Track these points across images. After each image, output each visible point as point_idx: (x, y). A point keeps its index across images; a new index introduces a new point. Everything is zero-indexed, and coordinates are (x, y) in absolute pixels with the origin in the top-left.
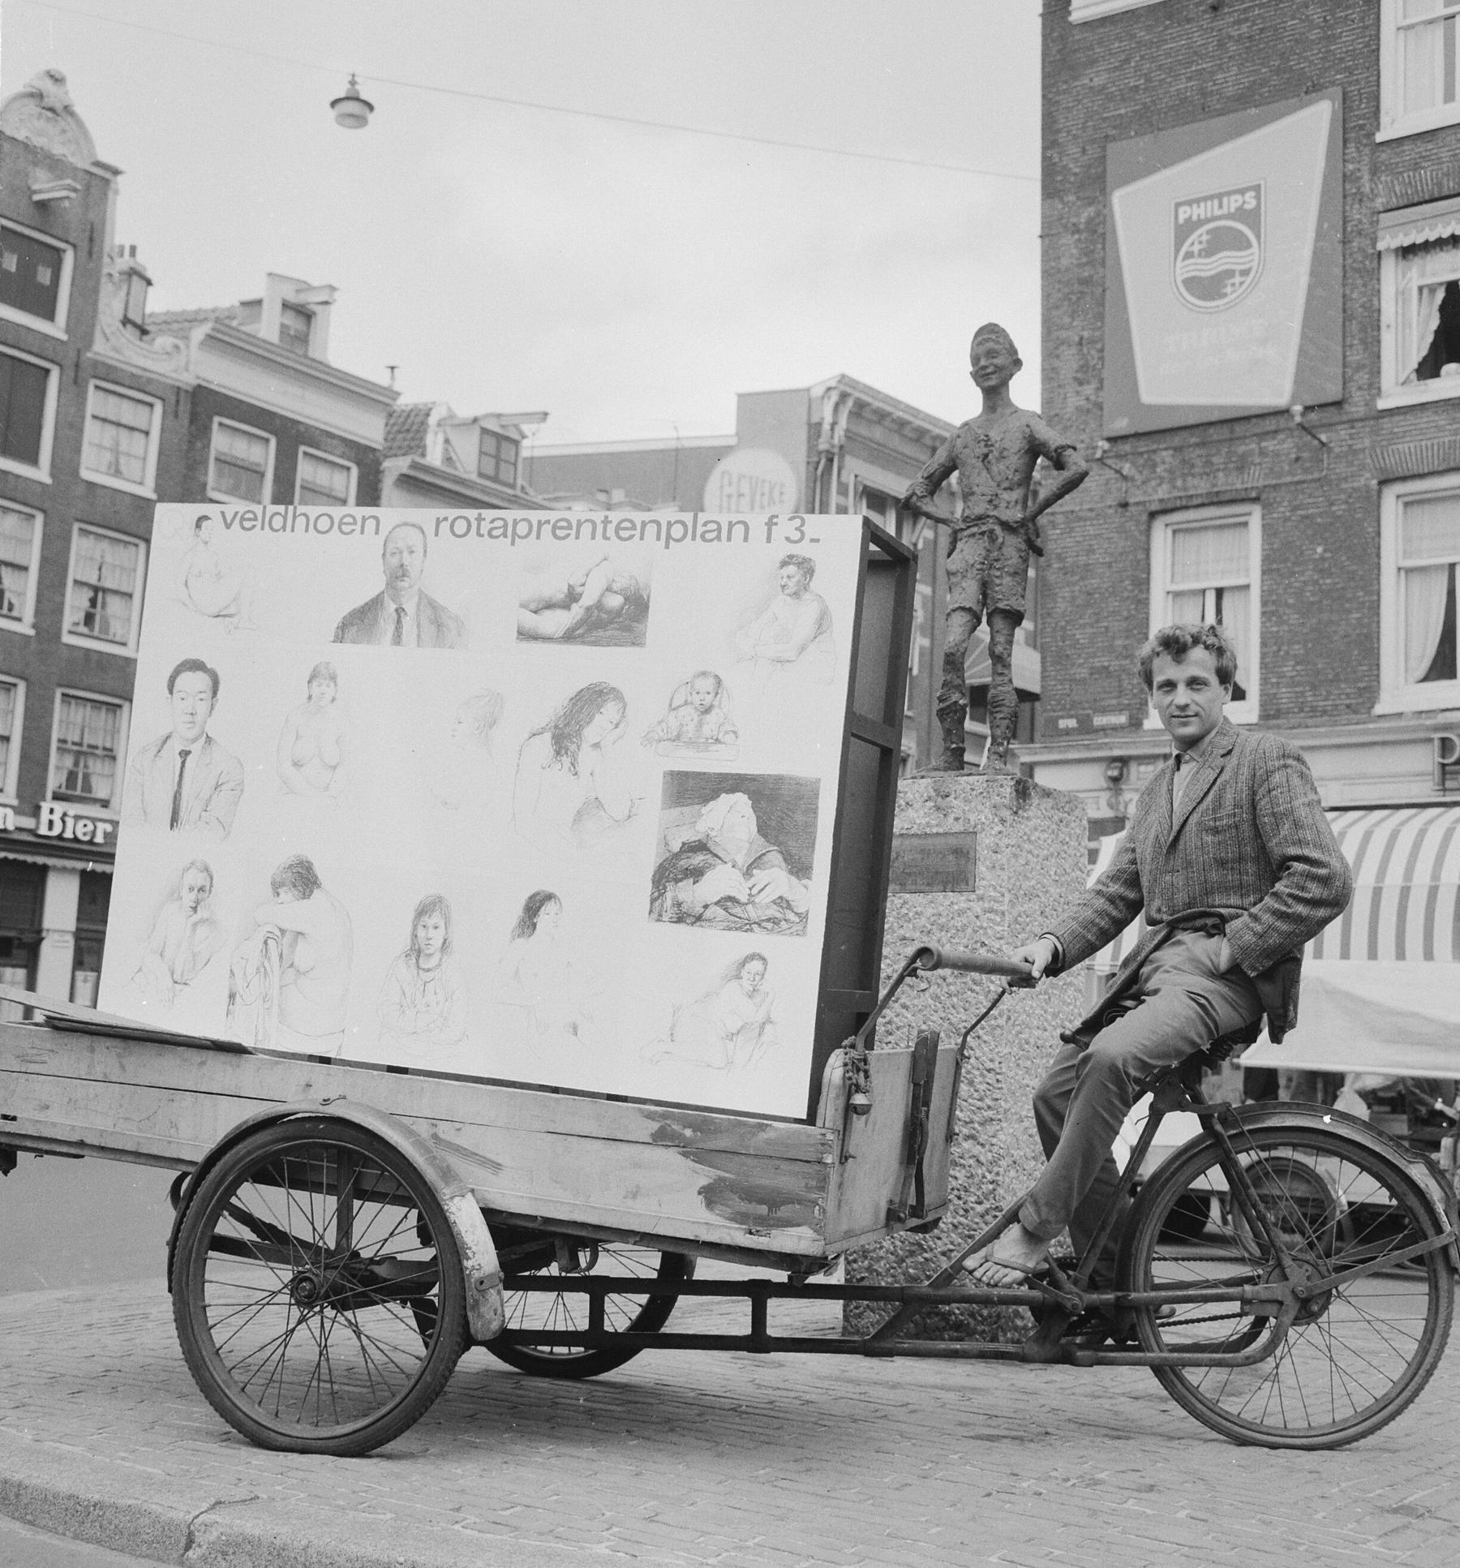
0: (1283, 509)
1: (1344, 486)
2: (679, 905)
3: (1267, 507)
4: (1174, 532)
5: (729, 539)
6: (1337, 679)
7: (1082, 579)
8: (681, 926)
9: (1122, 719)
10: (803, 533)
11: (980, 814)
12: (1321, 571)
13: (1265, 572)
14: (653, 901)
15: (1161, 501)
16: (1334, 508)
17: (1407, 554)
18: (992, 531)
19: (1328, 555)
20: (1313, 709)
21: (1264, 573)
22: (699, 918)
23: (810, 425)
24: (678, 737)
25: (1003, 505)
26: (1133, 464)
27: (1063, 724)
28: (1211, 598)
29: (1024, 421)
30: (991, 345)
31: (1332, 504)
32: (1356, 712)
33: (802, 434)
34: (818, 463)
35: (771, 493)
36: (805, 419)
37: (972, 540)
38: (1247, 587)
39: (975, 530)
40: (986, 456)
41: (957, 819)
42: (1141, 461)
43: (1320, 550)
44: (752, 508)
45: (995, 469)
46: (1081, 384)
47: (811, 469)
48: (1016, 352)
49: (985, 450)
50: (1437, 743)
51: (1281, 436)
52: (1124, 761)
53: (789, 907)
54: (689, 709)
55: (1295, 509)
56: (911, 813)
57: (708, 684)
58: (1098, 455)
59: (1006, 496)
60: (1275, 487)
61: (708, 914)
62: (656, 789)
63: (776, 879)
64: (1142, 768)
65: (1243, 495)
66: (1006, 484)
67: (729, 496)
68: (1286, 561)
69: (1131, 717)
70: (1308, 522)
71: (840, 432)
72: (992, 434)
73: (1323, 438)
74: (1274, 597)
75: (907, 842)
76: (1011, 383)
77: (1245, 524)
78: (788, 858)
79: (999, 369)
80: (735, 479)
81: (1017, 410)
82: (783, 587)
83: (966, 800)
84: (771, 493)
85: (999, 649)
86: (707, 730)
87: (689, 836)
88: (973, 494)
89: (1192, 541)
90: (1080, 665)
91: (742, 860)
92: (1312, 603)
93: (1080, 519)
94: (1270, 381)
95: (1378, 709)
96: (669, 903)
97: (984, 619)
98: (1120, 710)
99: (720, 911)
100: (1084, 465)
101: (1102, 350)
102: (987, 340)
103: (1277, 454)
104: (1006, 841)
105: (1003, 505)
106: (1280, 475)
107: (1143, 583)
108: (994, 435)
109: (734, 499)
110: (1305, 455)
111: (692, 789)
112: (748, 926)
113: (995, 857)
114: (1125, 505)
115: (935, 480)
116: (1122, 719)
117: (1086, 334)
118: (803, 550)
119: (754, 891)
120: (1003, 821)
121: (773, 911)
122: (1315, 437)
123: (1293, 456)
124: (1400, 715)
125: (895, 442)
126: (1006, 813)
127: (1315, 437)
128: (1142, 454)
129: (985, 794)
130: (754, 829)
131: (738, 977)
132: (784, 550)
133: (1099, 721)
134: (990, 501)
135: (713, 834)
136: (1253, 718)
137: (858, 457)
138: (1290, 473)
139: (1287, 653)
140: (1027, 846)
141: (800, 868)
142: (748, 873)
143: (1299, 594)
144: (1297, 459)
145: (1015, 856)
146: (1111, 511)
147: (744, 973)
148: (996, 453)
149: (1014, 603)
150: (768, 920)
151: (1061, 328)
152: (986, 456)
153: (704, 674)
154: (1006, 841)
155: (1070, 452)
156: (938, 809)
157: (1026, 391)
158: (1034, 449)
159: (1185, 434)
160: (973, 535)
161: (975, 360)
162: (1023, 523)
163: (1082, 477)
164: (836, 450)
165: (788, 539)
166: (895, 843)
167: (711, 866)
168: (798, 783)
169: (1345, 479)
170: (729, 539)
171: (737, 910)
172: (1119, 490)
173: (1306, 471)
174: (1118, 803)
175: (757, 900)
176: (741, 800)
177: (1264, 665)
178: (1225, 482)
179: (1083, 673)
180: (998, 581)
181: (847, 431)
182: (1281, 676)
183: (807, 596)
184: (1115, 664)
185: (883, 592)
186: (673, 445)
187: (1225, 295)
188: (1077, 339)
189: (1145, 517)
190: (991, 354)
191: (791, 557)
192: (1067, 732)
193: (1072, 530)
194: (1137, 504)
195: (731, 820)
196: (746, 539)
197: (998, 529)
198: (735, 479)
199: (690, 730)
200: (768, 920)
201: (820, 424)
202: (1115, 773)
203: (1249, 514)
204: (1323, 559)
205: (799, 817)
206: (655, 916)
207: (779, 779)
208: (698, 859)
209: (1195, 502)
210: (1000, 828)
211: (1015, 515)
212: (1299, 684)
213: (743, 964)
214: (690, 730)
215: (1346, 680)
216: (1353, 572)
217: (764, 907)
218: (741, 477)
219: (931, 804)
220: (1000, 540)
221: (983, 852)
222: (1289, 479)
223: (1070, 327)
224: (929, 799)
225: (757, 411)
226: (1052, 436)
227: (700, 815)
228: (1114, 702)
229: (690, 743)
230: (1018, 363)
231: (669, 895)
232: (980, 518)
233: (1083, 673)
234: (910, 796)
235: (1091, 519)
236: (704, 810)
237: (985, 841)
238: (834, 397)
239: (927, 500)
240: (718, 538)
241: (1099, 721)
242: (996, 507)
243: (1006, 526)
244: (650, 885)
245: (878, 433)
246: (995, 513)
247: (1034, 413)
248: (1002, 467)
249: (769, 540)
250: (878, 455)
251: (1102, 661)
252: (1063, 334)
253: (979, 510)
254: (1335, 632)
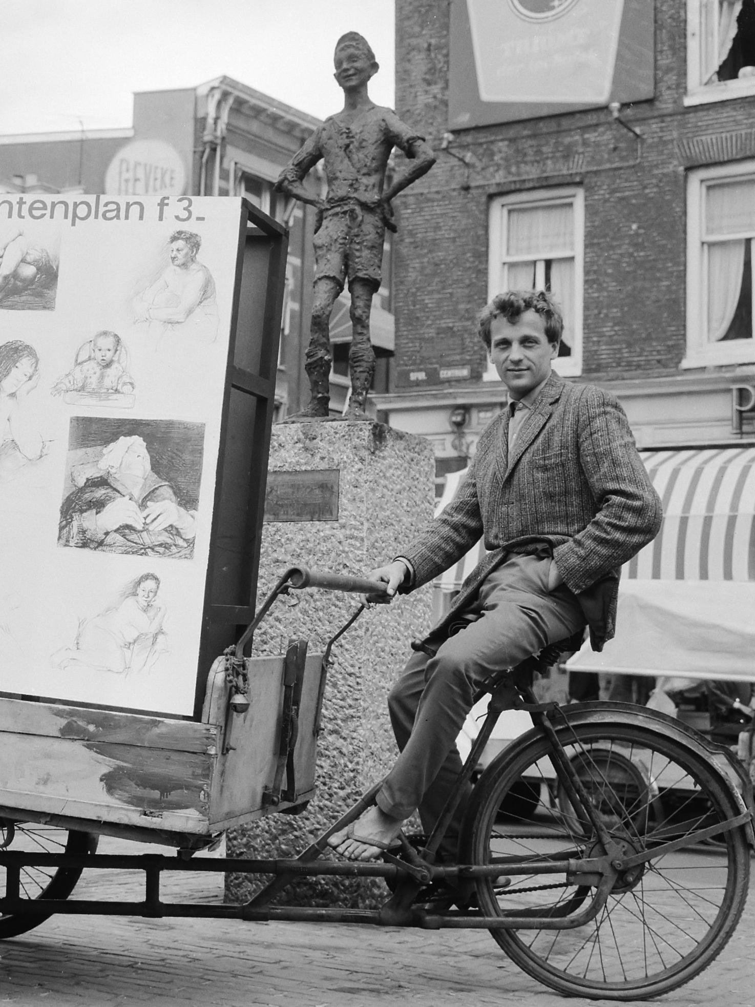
0: (603, 192)
1: (656, 172)
2: (84, 532)
3: (590, 190)
4: (510, 212)
5: (127, 218)
6: (649, 338)
7: (430, 251)
8: (86, 551)
9: (465, 372)
10: (190, 213)
11: (343, 454)
12: (636, 245)
14: (61, 528)
15: (498, 184)
16: (647, 191)
17: (709, 231)
18: (352, 211)
19: (642, 231)
20: (629, 364)
21: (586, 246)
22: (101, 544)
23: (196, 120)
24: (83, 388)
25: (362, 188)
26: (474, 153)
29: (380, 117)
30: (352, 51)
31: (645, 188)
32: (665, 366)
33: (190, 127)
34: (203, 152)
35: (162, 178)
36: (191, 114)
37: (336, 219)
38: (572, 259)
39: (338, 209)
40: (348, 146)
41: (322, 458)
42: (481, 151)
43: (634, 227)
44: (147, 191)
45: (355, 157)
46: (429, 83)
47: (197, 157)
48: (373, 57)
49: (347, 141)
50: (735, 393)
51: (601, 129)
53: (178, 534)
54: (92, 364)
55: (613, 191)
56: (283, 453)
57: (109, 342)
58: (444, 145)
59: (364, 180)
60: (596, 173)
61: (109, 540)
62: (64, 432)
63: (167, 509)
64: (482, 415)
65: (569, 180)
66: (365, 171)
67: (127, 181)
68: (605, 236)
69: (472, 371)
70: (624, 203)
71: (222, 125)
72: (352, 127)
73: (638, 130)
74: (595, 268)
75: (280, 478)
76: (369, 83)
77: (570, 205)
78: (177, 492)
79: (358, 71)
80: (132, 166)
81: (374, 107)
82: (173, 259)
83: (331, 443)
84: (162, 178)
85: (359, 312)
86: (108, 382)
87: (92, 472)
88: (336, 178)
89: (524, 220)
90: (429, 326)
91: (138, 493)
92: (628, 272)
93: (428, 200)
94: (593, 84)
95: (685, 364)
96: (75, 530)
97: (346, 287)
98: (463, 365)
99: (119, 538)
100: (431, 154)
101: (447, 55)
102: (348, 47)
103: (597, 145)
104: (365, 477)
105: (362, 188)
106: (600, 163)
107: (483, 256)
108: (355, 128)
109: (131, 184)
110: (622, 145)
111: (94, 433)
112: (143, 550)
113: (355, 491)
114: (467, 188)
115: (303, 167)
117: (433, 41)
118: (190, 227)
119: (148, 521)
120: (362, 460)
121: (165, 538)
122: (630, 130)
123: (612, 146)
124: (703, 369)
125: (270, 134)
126: (365, 454)
127: (630, 130)
128: (481, 144)
129: (347, 437)
130: (149, 467)
131: (135, 594)
132: (171, 226)
133: (445, 374)
134: (351, 185)
135: (113, 471)
136: (578, 372)
137: (237, 147)
138: (610, 161)
139: (606, 315)
140: (383, 482)
141: (188, 501)
142: (143, 505)
144: (615, 149)
145: (373, 490)
146: (455, 193)
147: (140, 591)
148: (356, 144)
149: (372, 273)
150: (160, 545)
151: (412, 36)
152: (348, 146)
153: (105, 333)
154: (365, 477)
155: (419, 142)
156: (306, 449)
157: (382, 90)
158: (389, 140)
159: (518, 127)
160: (337, 214)
161: (338, 63)
162: (379, 204)
163: (431, 163)
164: (219, 141)
165: (177, 217)
166: (270, 479)
167: (111, 499)
168: (186, 427)
169: (656, 166)
170: (127, 218)
171: (134, 537)
172: (462, 175)
173: (622, 159)
174: (461, 445)
175: (151, 528)
176: (137, 443)
177: (586, 326)
178: (554, 168)
179: (431, 332)
180: (357, 254)
181: (228, 124)
182: (601, 335)
183: (194, 266)
184: (458, 326)
185: (259, 264)
186: (78, 136)
187: (553, 8)
188: (426, 45)
189: (484, 199)
190: (352, 58)
191: (180, 233)
192: (418, 383)
193: (422, 209)
194: (478, 187)
195: (129, 459)
196: (141, 218)
197: (358, 209)
198: (132, 166)
199: (93, 382)
200: (160, 545)
201: (204, 119)
202: (459, 419)
203: (574, 196)
204: (637, 235)
205: (187, 457)
206: (63, 541)
207: (170, 424)
208: (100, 493)
209: (531, 185)
210: (359, 466)
211: (373, 197)
212: (617, 342)
213: (139, 583)
214: (93, 382)
215: (657, 339)
216: (664, 246)
217: (156, 534)
218: (137, 164)
219: (300, 445)
220: (360, 218)
221: (345, 487)
222: (608, 166)
223: (419, 35)
224: (299, 441)
225: (152, 107)
226: (405, 130)
227: (102, 455)
228: (458, 357)
229: (93, 393)
230: (375, 66)
231: (75, 524)
232: (342, 199)
233: (431, 332)
234: (282, 438)
235: (438, 200)
236: (105, 451)
237: (347, 477)
238: (217, 95)
239: (297, 184)
240: (118, 217)
241: (445, 374)
242: (356, 190)
243: (364, 206)
244: (59, 515)
245: (255, 127)
246: (355, 195)
247: (389, 110)
248: (361, 155)
249: (161, 219)
250: (255, 145)
251: (447, 322)
252: (414, 41)
253: (342, 192)
254: (648, 298)
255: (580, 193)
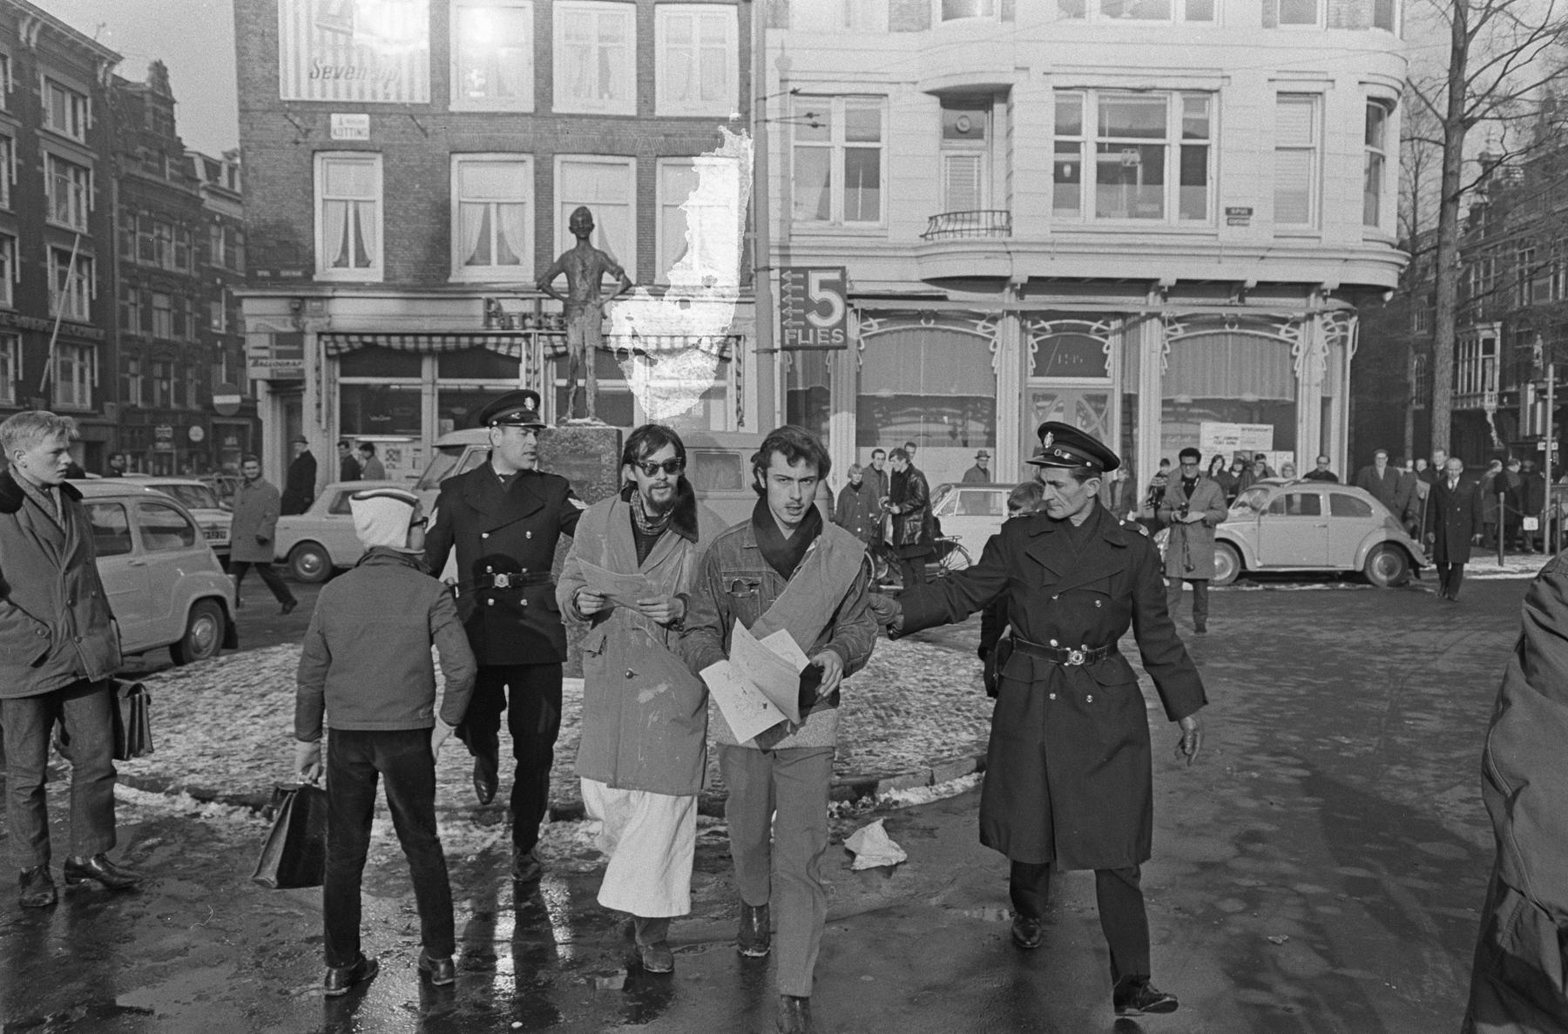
3: (386, 158)
13: (386, 195)
27: (260, 273)
28: (351, 206)
52: (303, 298)
55: (402, 160)
95: (451, 280)
98: (296, 268)
114: (297, 143)
116: (299, 274)
143: (406, 211)
177: (385, 249)
179: (273, 243)
192: (263, 278)
241: (285, 273)
255: (379, 157)
